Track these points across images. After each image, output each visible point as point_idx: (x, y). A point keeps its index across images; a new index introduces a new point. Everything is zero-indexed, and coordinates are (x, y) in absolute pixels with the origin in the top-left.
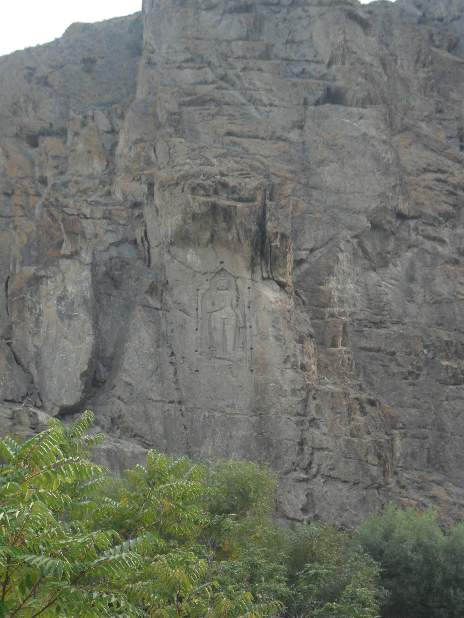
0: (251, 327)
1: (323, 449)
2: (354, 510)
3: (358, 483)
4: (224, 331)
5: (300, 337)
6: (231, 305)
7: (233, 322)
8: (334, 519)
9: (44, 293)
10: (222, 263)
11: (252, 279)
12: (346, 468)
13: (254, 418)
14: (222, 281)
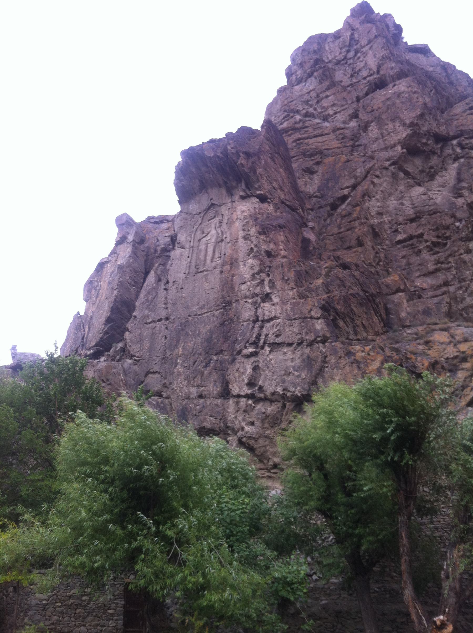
0: (226, 238)
1: (271, 319)
2: (297, 371)
3: (302, 343)
4: (206, 250)
5: (263, 229)
6: (215, 228)
7: (213, 240)
8: (276, 386)
9: (104, 273)
10: (211, 199)
11: (232, 202)
12: (290, 331)
13: (218, 312)
14: (211, 213)
